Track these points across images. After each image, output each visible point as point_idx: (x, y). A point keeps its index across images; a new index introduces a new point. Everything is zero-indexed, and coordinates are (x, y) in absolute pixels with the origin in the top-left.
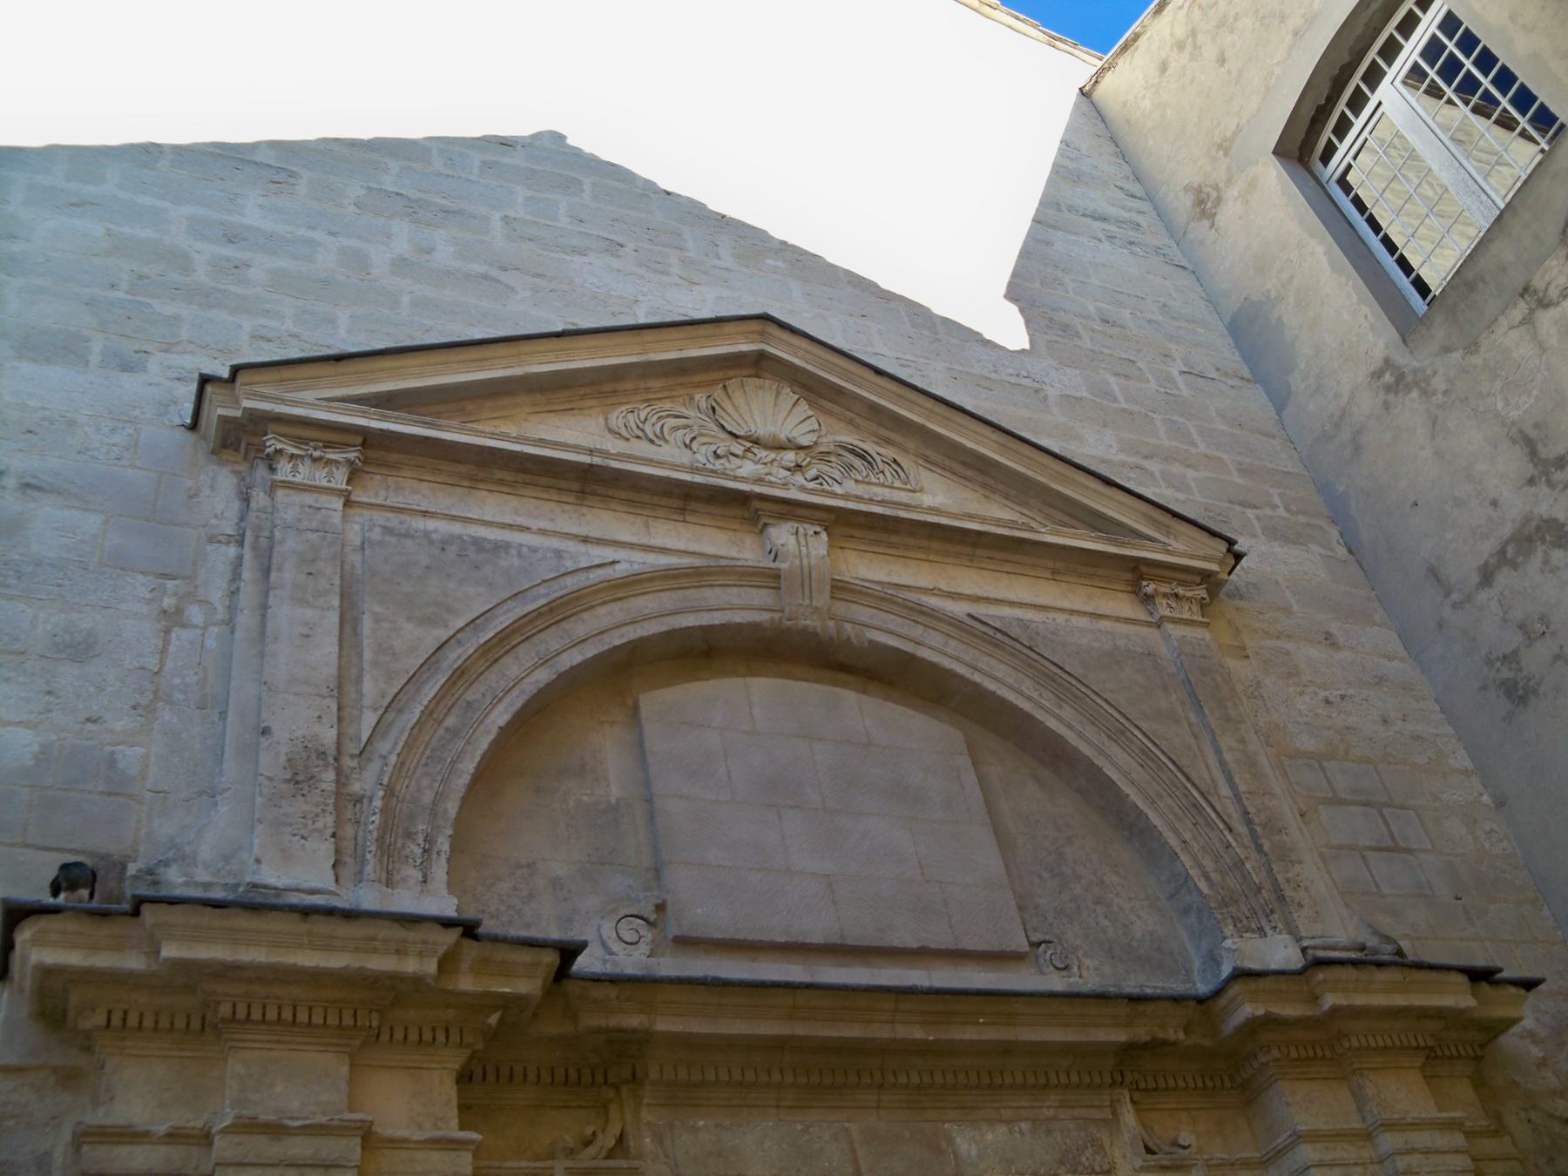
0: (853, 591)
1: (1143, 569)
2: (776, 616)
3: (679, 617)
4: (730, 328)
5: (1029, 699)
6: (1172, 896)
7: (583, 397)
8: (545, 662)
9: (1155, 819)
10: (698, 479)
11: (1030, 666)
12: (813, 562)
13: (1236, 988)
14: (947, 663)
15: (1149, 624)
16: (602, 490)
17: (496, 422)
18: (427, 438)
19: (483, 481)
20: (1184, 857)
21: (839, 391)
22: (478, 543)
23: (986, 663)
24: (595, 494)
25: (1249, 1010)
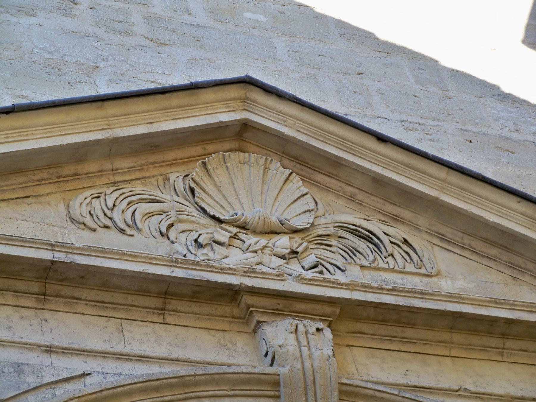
4: (208, 95)
7: (40, 182)
10: (179, 273)
16: (66, 291)
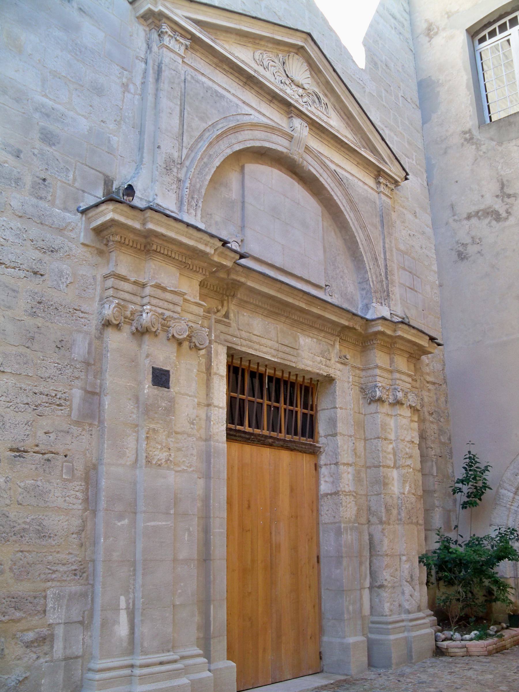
0: (309, 150)
1: (382, 173)
2: (288, 151)
3: (264, 142)
4: (298, 34)
5: (344, 206)
6: (360, 283)
7: (249, 42)
8: (230, 146)
9: (365, 259)
10: (281, 94)
11: (347, 195)
12: (303, 137)
13: (380, 321)
14: (326, 186)
15: (376, 192)
16: (251, 85)
17: (224, 42)
18: (211, 46)
19: (219, 67)
20: (369, 274)
21: (320, 71)
22: (216, 92)
23: (336, 189)
24: (249, 85)
25: (380, 328)
